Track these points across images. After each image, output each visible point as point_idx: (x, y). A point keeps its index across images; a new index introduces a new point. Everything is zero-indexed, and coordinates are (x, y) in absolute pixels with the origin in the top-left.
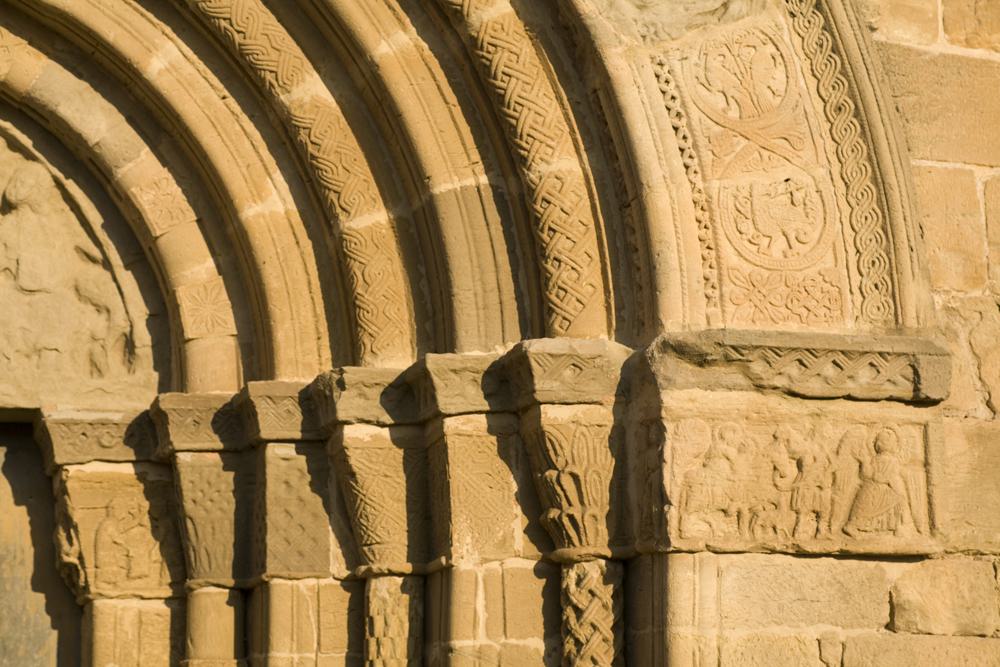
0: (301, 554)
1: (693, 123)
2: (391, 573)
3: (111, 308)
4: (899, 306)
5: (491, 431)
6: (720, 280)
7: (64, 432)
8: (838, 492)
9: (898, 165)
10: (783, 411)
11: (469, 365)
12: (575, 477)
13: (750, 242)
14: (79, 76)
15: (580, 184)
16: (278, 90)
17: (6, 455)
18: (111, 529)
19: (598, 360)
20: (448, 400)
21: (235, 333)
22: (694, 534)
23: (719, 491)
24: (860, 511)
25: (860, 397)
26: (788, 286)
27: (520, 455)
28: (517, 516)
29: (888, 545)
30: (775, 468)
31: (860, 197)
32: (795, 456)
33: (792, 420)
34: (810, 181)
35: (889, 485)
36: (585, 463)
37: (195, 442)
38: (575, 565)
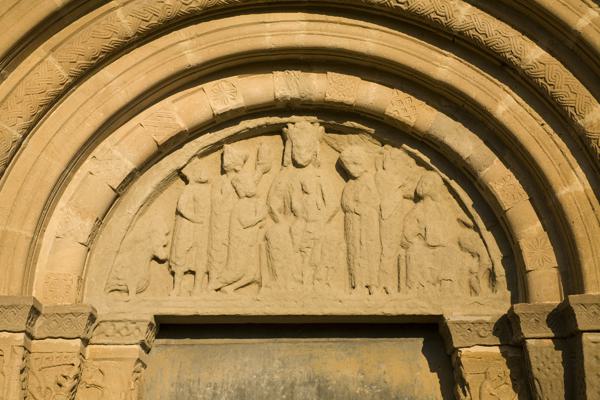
14: (456, 119)
16: (576, 117)
18: (488, 386)
21: (557, 265)
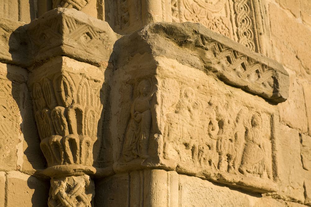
8: (237, 145)
10: (216, 88)
11: (4, 23)
12: (79, 113)
19: (102, 35)
23: (185, 130)
24: (248, 159)
27: (26, 99)
28: (20, 141)
36: (85, 104)
38: (67, 179)
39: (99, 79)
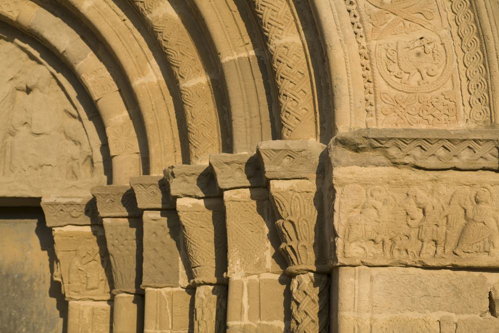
0: (162, 273)
1: (360, 7)
2: (205, 284)
3: (81, 142)
4: (492, 112)
5: (252, 197)
6: (375, 100)
7: (51, 209)
9: (493, 24)
10: (412, 178)
11: (235, 159)
13: (396, 77)
14: (56, 16)
15: (300, 51)
16: (146, 12)
17: (38, 224)
18: (77, 262)
19: (303, 153)
20: (224, 181)
21: (138, 151)
22: (354, 255)
23: (369, 228)
24: (464, 240)
25: (463, 168)
26: (420, 103)
29: (484, 260)
30: (407, 214)
31: (469, 45)
32: (421, 206)
33: (418, 184)
34: (437, 38)
35: (484, 223)
36: (299, 214)
37: (112, 212)
38: (297, 277)
39: (312, 190)
